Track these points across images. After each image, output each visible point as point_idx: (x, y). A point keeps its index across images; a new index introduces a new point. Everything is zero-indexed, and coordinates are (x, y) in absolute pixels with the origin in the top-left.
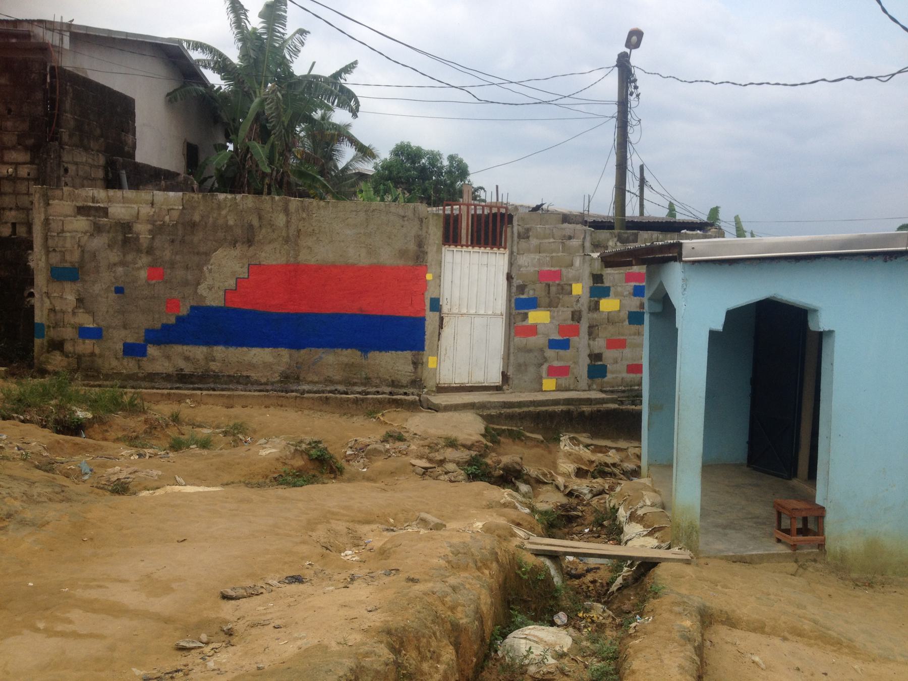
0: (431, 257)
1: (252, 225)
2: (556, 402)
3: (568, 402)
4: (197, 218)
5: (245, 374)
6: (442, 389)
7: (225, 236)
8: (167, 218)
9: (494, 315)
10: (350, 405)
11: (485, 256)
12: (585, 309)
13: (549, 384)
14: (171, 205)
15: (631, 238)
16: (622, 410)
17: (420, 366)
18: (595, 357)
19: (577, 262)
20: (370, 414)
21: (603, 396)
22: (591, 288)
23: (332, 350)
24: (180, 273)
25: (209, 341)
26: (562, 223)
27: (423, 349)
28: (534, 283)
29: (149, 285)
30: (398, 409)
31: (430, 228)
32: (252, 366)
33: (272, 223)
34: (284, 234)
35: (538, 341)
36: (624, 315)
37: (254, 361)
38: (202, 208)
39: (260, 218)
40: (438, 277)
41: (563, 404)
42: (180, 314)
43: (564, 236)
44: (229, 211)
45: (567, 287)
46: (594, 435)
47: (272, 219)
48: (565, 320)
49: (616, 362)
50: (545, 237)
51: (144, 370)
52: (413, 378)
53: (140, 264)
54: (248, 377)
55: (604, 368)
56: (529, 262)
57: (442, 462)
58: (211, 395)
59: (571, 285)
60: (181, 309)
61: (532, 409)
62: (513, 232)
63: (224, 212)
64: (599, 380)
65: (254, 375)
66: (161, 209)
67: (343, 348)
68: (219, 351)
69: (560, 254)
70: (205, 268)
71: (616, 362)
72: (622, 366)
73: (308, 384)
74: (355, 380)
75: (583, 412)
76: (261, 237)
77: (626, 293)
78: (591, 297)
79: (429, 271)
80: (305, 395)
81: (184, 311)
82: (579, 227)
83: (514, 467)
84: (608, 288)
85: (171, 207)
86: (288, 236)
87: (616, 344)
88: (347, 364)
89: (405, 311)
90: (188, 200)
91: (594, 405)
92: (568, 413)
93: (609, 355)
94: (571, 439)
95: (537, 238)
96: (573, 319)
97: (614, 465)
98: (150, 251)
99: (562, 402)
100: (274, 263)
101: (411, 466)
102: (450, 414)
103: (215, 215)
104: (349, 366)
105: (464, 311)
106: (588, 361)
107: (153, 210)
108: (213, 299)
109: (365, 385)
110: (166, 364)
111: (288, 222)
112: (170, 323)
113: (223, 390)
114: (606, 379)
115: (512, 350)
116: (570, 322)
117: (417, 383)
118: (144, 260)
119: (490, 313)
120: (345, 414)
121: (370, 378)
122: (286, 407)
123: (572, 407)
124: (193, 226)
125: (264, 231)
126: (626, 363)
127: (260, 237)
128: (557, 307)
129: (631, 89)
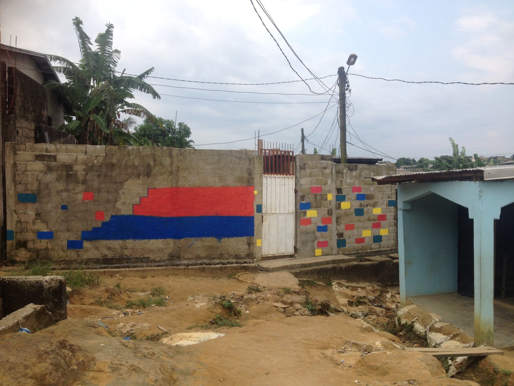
0: (256, 181)
1: (150, 165)
2: (327, 263)
3: (333, 262)
4: (115, 161)
5: (146, 256)
7: (133, 172)
8: (95, 162)
9: (289, 213)
10: (218, 272)
12: (334, 208)
13: (318, 252)
14: (98, 153)
15: (354, 168)
16: (360, 265)
17: (252, 245)
18: (340, 235)
19: (329, 182)
20: (230, 277)
21: (347, 257)
22: (337, 196)
23: (200, 238)
24: (104, 195)
25: (123, 237)
26: (321, 160)
27: (253, 235)
29: (84, 203)
30: (247, 273)
31: (255, 164)
32: (151, 251)
33: (161, 163)
34: (169, 169)
35: (312, 227)
36: (353, 211)
37: (152, 248)
38: (118, 155)
39: (154, 160)
40: (261, 192)
41: (331, 264)
42: (105, 221)
43: (322, 167)
44: (135, 156)
45: (325, 196)
46: (349, 280)
47: (162, 161)
48: (324, 215)
50: (313, 169)
51: (81, 257)
52: (248, 252)
53: (78, 190)
54: (148, 258)
55: (345, 240)
56: (306, 182)
57: (292, 304)
58: (131, 271)
59: (327, 195)
60: (105, 217)
61: (316, 267)
62: (296, 165)
63: (132, 157)
64: (342, 248)
65: (152, 256)
66: (91, 156)
67: (206, 237)
68: (130, 243)
69: (320, 178)
70: (120, 192)
72: (353, 240)
73: (185, 260)
74: (214, 256)
75: (342, 267)
76: (155, 172)
77: (353, 198)
78: (336, 201)
79: (255, 189)
80: (189, 267)
81: (107, 219)
82: (329, 162)
83: (327, 303)
85: (98, 155)
86: (172, 171)
87: (349, 227)
88: (209, 246)
89: (243, 213)
90: (109, 150)
91: (346, 263)
92: (334, 268)
93: (347, 233)
94: (338, 284)
95: (309, 169)
97: (364, 297)
98: (84, 182)
99: (330, 263)
100: (163, 187)
101: (275, 308)
102: (275, 274)
103: (126, 159)
104: (210, 247)
105: (273, 212)
106: (336, 237)
107: (86, 156)
108: (126, 210)
109: (220, 258)
110: (96, 253)
111: (172, 162)
112: (98, 226)
113: (134, 267)
114: (346, 248)
115: (298, 233)
116: (327, 216)
117: (250, 256)
118: (81, 188)
119: (287, 212)
120: (215, 277)
121: (222, 254)
122: (179, 275)
123: (335, 265)
124: (112, 166)
125: (157, 168)
126: (355, 238)
127: (155, 171)
128: (320, 207)
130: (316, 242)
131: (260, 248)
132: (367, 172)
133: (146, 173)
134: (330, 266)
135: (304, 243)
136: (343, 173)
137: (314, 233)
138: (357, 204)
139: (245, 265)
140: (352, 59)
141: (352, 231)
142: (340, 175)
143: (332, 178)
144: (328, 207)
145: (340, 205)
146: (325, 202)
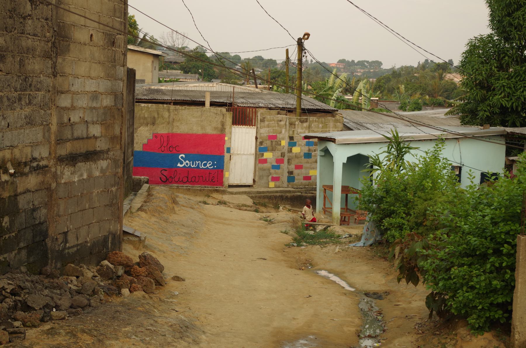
0: (227, 130)
2: (277, 192)
3: (281, 192)
6: (230, 186)
9: (250, 154)
11: (247, 129)
12: (286, 151)
13: (272, 184)
15: (305, 120)
18: (290, 173)
19: (283, 131)
28: (266, 140)
34: (168, 120)
36: (302, 154)
39: (158, 114)
40: (230, 138)
41: (280, 193)
43: (278, 120)
46: (293, 206)
48: (278, 157)
49: (298, 175)
50: (271, 121)
55: (294, 177)
56: (265, 132)
59: (281, 141)
63: (143, 112)
64: (292, 183)
71: (298, 175)
75: (287, 196)
77: (303, 145)
79: (226, 136)
84: (296, 142)
87: (299, 167)
92: (282, 196)
93: (296, 172)
96: (281, 156)
106: (287, 174)
111: (169, 115)
114: (294, 183)
115: (257, 170)
120: (196, 196)
123: (283, 194)
125: (159, 119)
126: (303, 175)
127: (157, 122)
129: (303, 54)
130: (270, 177)
131: (228, 178)
132: (317, 123)
133: (152, 123)
134: (278, 194)
135: (261, 177)
136: (295, 125)
137: (269, 170)
138: (306, 149)
139: (217, 189)
140: (306, 37)
141: (301, 170)
142: (293, 126)
143: (286, 128)
144: (281, 151)
145: (291, 149)
146: (279, 147)
